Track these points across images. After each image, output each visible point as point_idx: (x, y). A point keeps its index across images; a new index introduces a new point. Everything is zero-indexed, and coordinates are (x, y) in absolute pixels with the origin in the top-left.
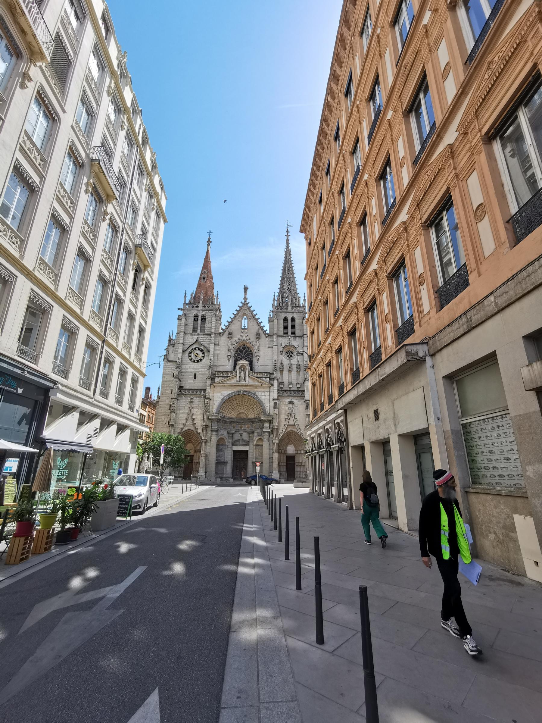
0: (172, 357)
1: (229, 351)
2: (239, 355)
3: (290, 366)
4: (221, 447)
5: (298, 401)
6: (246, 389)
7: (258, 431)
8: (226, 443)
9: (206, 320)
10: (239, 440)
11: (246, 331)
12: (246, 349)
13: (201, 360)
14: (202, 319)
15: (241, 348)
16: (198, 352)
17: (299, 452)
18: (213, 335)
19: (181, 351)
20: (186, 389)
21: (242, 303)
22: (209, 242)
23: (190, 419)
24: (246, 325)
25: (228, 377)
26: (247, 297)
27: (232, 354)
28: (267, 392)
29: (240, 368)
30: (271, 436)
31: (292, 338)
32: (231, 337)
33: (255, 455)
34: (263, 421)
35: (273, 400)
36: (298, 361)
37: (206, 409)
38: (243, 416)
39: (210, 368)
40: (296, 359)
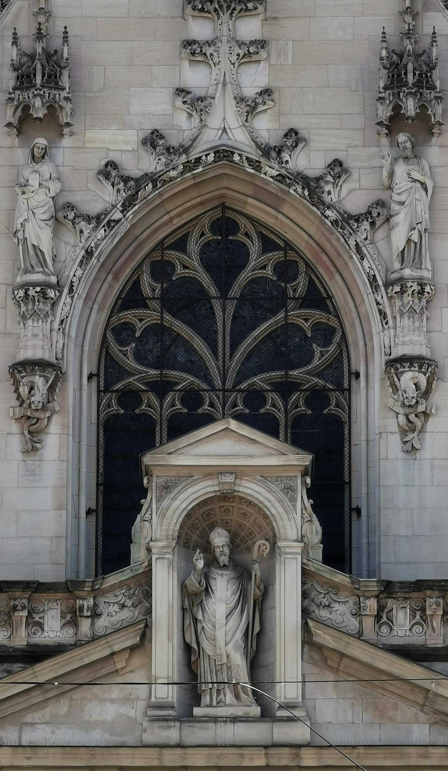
2: (160, 348)
12: (258, 264)
15: (190, 265)
25: (35, 655)
27: (71, 337)
29: (193, 535)
32: (54, 123)
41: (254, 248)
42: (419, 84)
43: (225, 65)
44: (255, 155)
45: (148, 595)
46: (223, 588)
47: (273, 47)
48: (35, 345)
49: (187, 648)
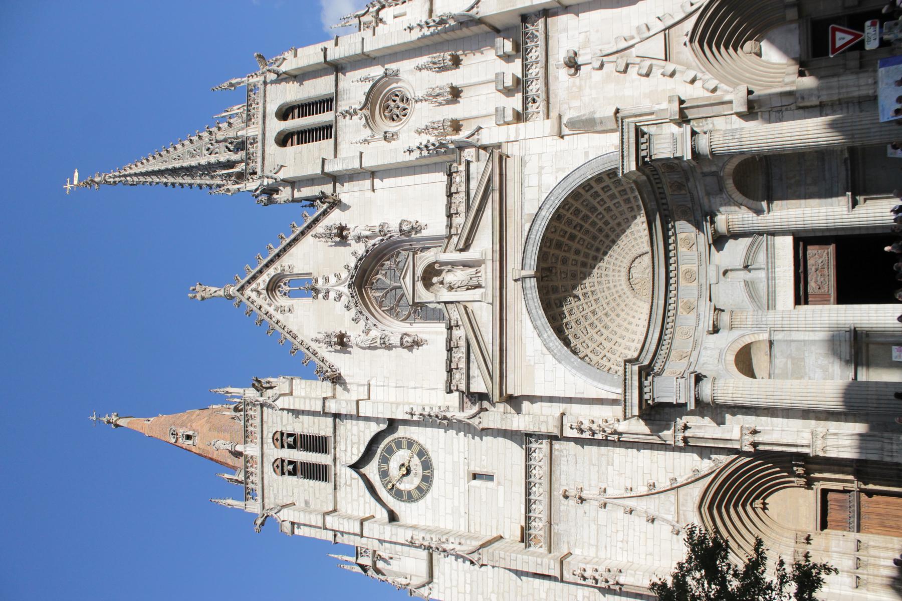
3: (433, 96)
5: (563, 37)
7: (701, 193)
8: (765, 336)
9: (290, 430)
11: (321, 281)
14: (290, 446)
20: (528, 519)
31: (343, 106)
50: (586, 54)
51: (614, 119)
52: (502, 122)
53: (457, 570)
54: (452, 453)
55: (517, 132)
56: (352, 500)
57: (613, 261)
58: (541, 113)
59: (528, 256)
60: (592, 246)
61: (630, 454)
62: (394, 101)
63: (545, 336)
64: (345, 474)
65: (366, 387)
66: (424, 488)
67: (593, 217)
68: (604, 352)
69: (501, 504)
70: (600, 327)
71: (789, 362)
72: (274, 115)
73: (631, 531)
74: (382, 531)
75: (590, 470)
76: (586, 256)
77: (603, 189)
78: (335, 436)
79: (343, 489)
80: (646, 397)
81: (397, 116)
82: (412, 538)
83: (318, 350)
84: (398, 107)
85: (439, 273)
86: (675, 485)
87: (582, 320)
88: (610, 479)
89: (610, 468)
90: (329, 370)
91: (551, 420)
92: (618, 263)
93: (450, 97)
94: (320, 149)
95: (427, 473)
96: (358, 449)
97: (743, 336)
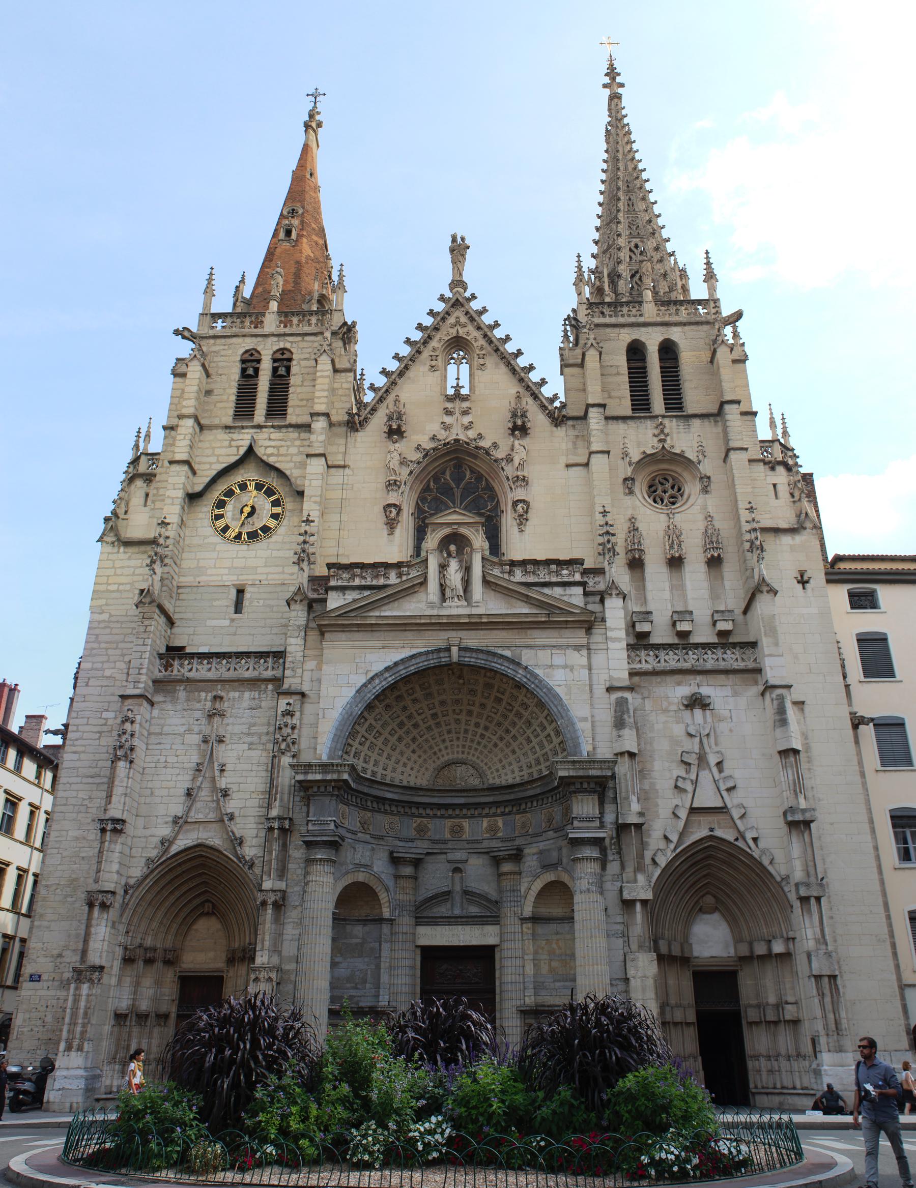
0: (139, 524)
1: (392, 485)
3: (673, 536)
4: (359, 930)
5: (728, 691)
6: (473, 639)
7: (542, 845)
8: (386, 913)
9: (294, 370)
10: (445, 896)
11: (465, 405)
13: (266, 529)
14: (275, 370)
16: (252, 497)
17: (760, 949)
18: (320, 424)
19: (180, 494)
20: (192, 656)
21: (442, 298)
22: (312, 124)
23: (204, 794)
24: (465, 381)
26: (465, 278)
28: (577, 648)
30: (613, 867)
31: (671, 425)
33: (529, 969)
34: (569, 787)
35: (609, 689)
36: (709, 518)
37: (282, 739)
38: (465, 777)
39: (303, 557)
40: (696, 509)
41: (468, 473)
42: (522, 416)
43: (457, 414)
44: (467, 440)
45: (427, 567)
46: (454, 565)
47: (473, 409)
48: (392, 501)
49: (441, 585)
50: (705, 717)
51: (624, 750)
52: (634, 619)
53: (134, 574)
54: (266, 566)
55: (618, 640)
56: (213, 448)
57: (475, 745)
58: (639, 666)
59: (474, 655)
60: (490, 722)
61: (260, 768)
62: (673, 488)
63: (387, 675)
64: (243, 439)
65: (342, 463)
66: (227, 534)
67: (520, 723)
68: (371, 737)
69: (210, 623)
70: (400, 732)
71: (358, 941)
72: (666, 337)
73: (177, 771)
74: (177, 486)
75: (243, 724)
76: (480, 715)
77: (549, 735)
78: (286, 426)
79: (226, 437)
80: (315, 789)
81: (655, 491)
82: (168, 524)
83: (385, 403)
84: (665, 492)
85: (460, 551)
86: (226, 819)
87: (408, 713)
88: (234, 746)
89: (246, 746)
90: (361, 418)
91: (298, 680)
92: (472, 752)
93: (669, 556)
94: (620, 398)
95: (244, 536)
96: (272, 455)
97: (387, 890)
